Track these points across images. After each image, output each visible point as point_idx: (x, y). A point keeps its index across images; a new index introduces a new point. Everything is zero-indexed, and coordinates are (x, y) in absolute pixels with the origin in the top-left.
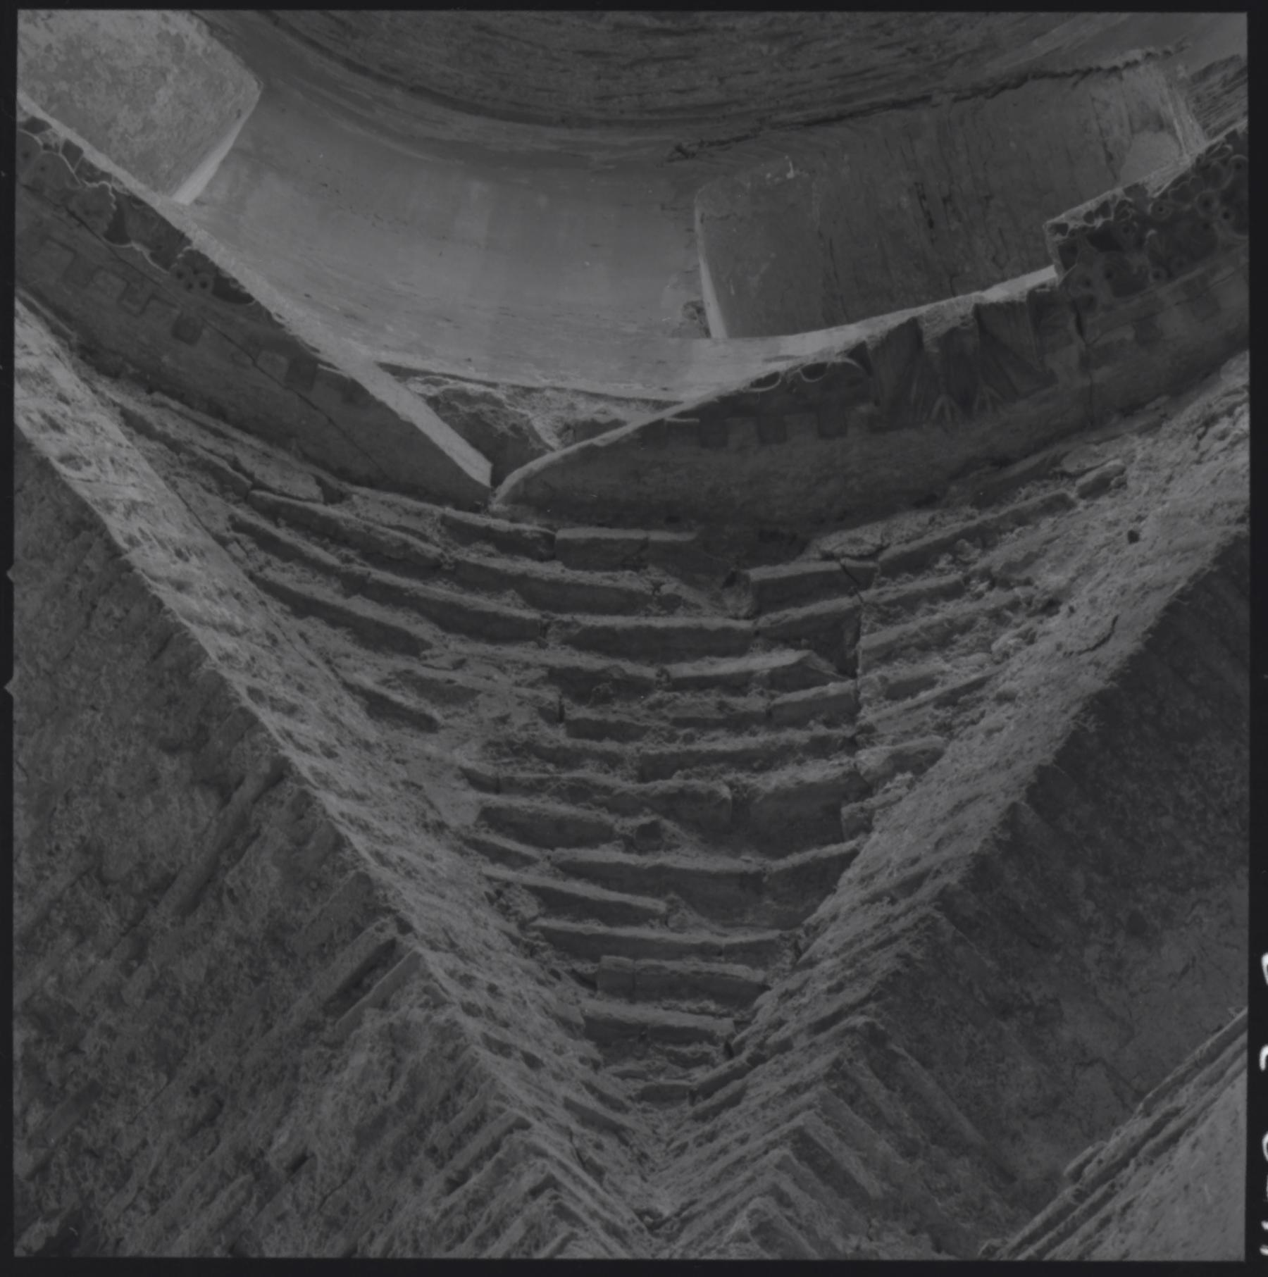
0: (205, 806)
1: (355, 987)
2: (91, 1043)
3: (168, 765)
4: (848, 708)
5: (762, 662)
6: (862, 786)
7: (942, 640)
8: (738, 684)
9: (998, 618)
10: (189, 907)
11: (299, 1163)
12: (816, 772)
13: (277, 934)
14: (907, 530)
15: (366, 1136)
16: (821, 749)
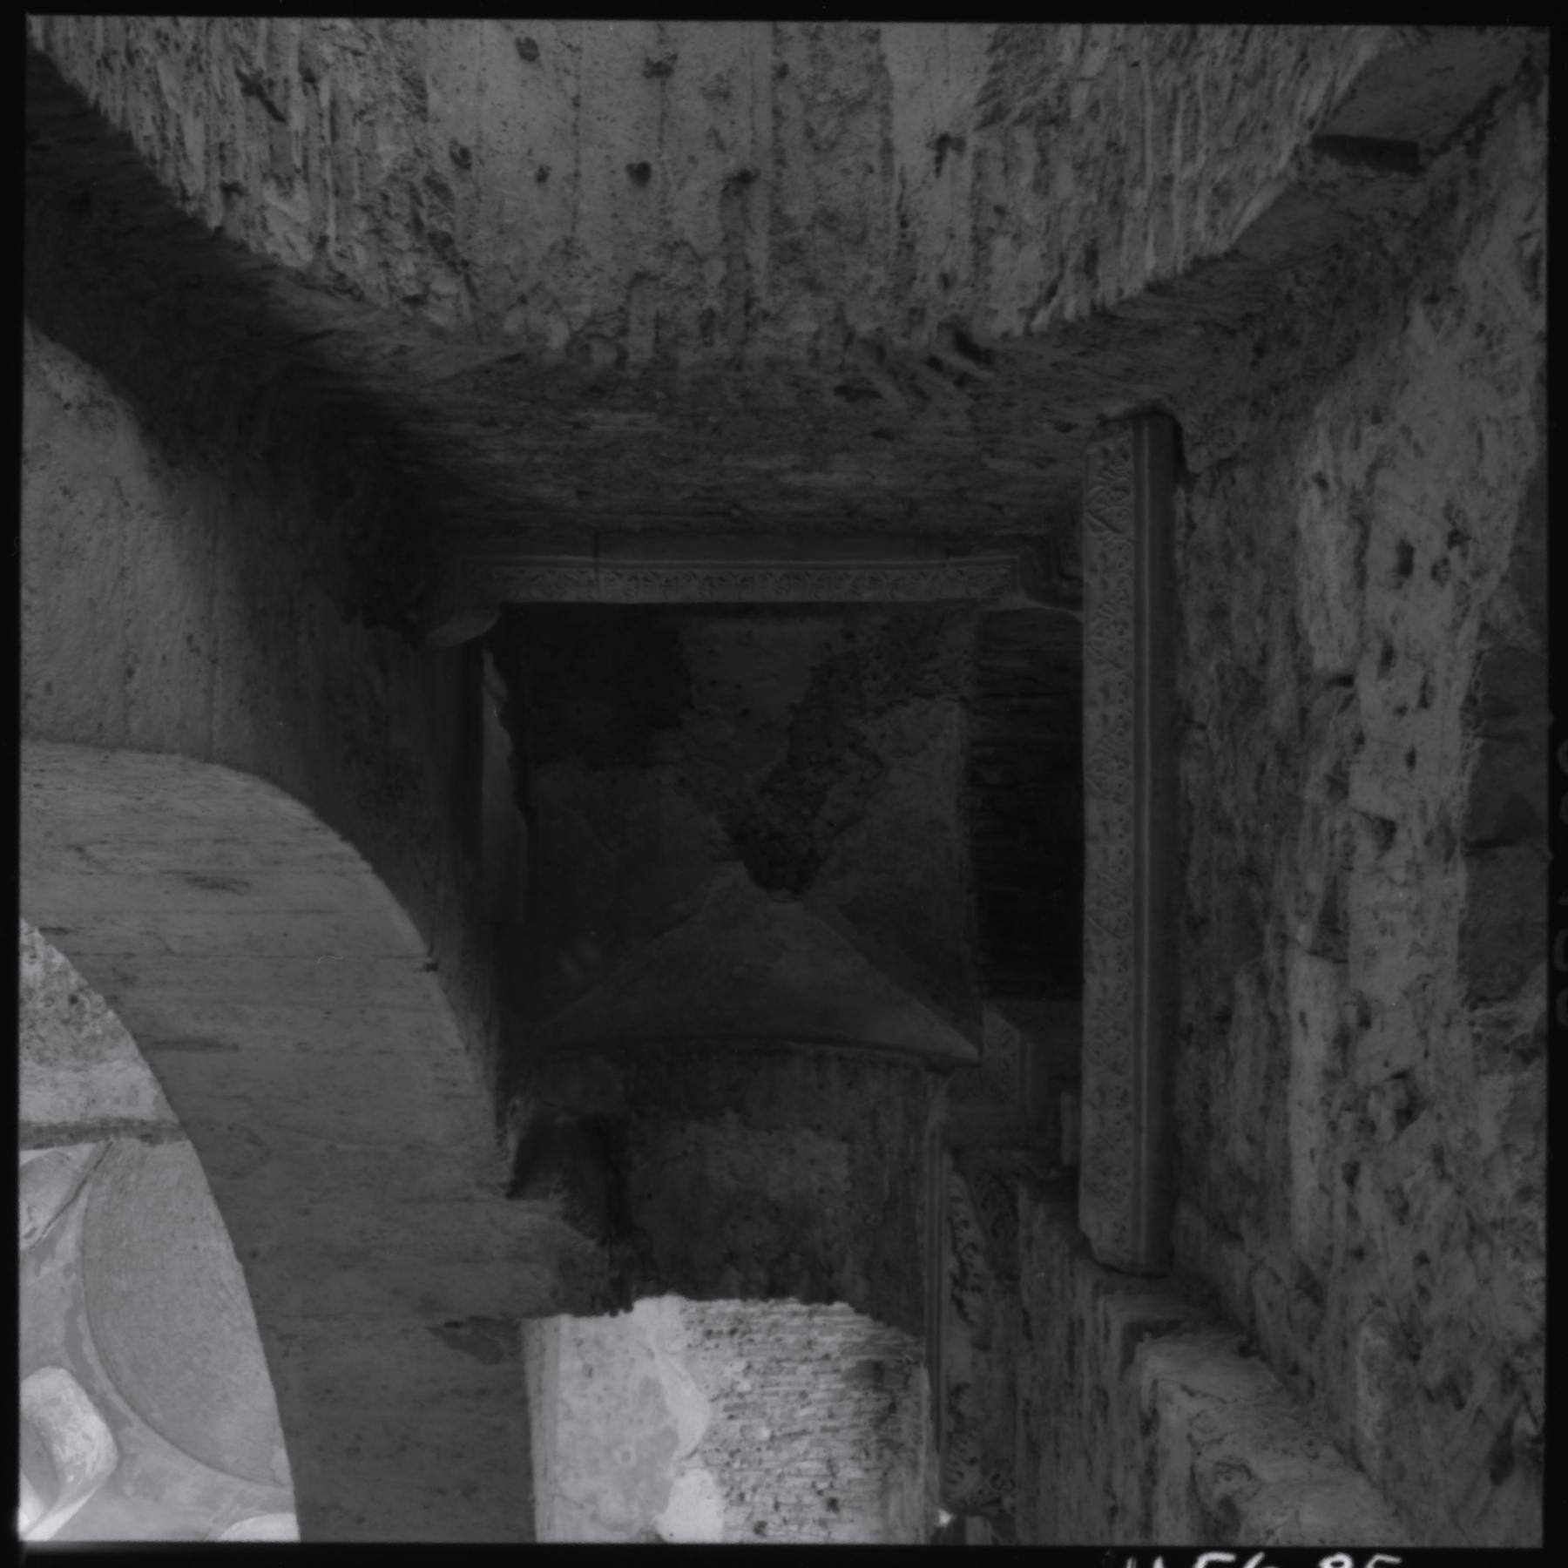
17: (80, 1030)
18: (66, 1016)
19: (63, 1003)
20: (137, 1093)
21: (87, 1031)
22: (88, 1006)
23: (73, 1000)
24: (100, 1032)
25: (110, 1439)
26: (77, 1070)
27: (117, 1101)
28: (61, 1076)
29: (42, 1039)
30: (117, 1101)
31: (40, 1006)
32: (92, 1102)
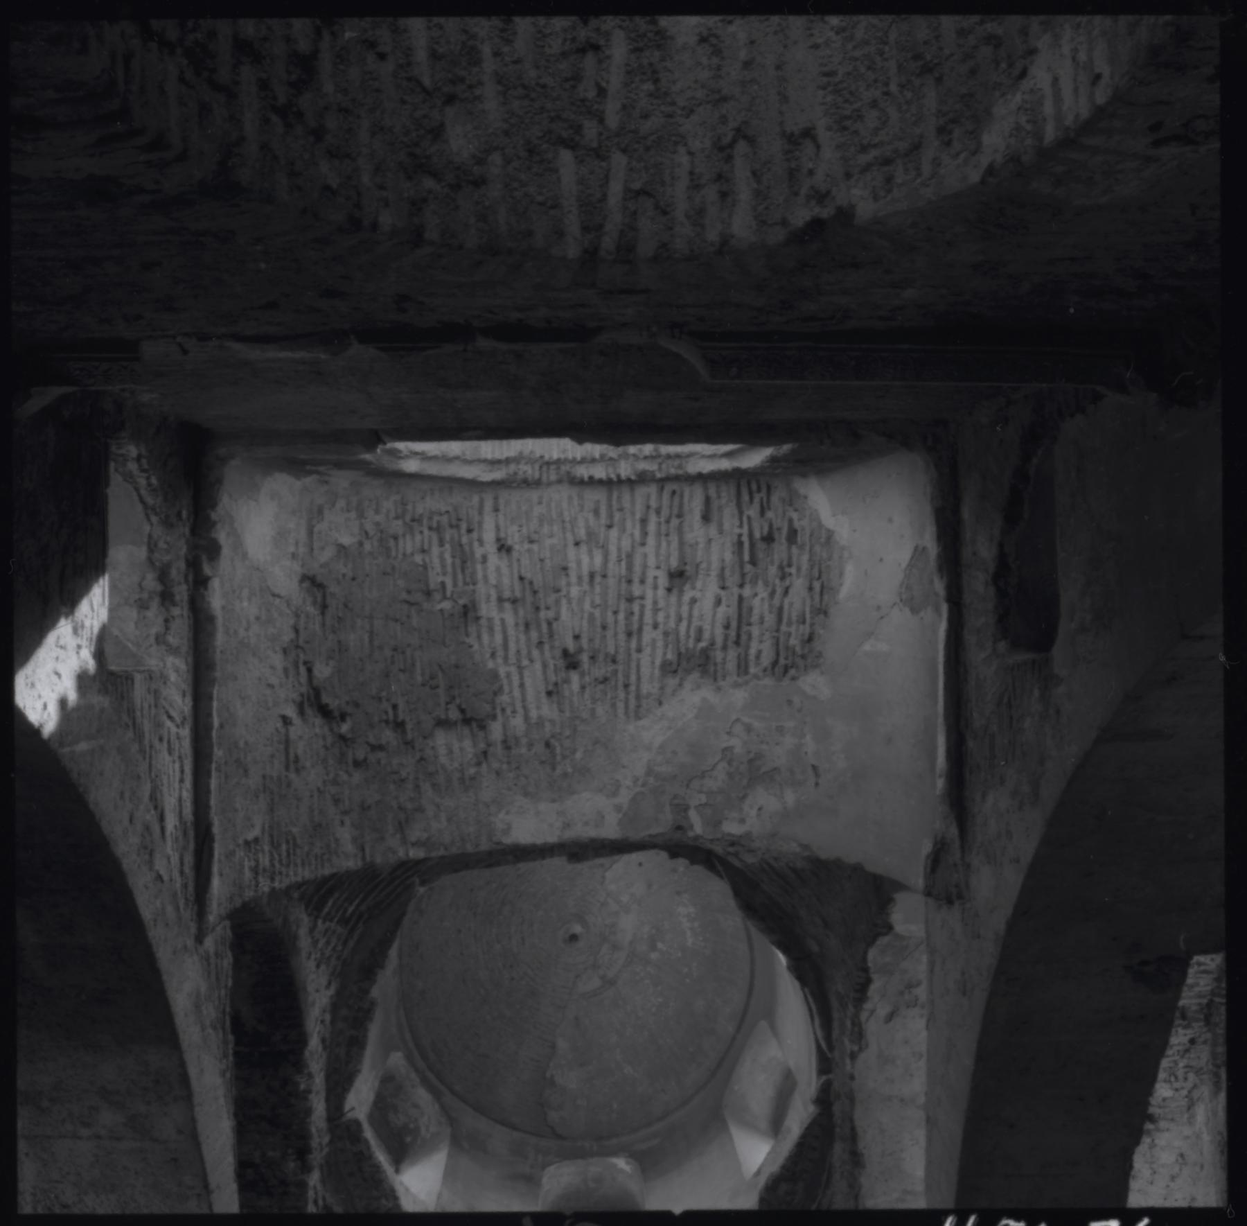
0: (413, 839)
1: (363, 850)
2: (392, 787)
3: (425, 835)
4: (331, 920)
5: (351, 909)
6: (317, 917)
7: (328, 943)
8: (351, 904)
9: (323, 954)
10: (400, 823)
11: (342, 823)
12: (326, 910)
13: (383, 839)
14: (351, 944)
15: (337, 840)
16: (329, 913)
17: (554, 769)
18: (543, 758)
19: (539, 748)
20: (603, 817)
21: (559, 771)
22: (558, 750)
23: (548, 745)
24: (570, 770)
25: (437, 1106)
26: (554, 801)
27: (586, 824)
28: (542, 806)
29: (526, 777)
30: (586, 824)
31: (524, 750)
32: (567, 825)
